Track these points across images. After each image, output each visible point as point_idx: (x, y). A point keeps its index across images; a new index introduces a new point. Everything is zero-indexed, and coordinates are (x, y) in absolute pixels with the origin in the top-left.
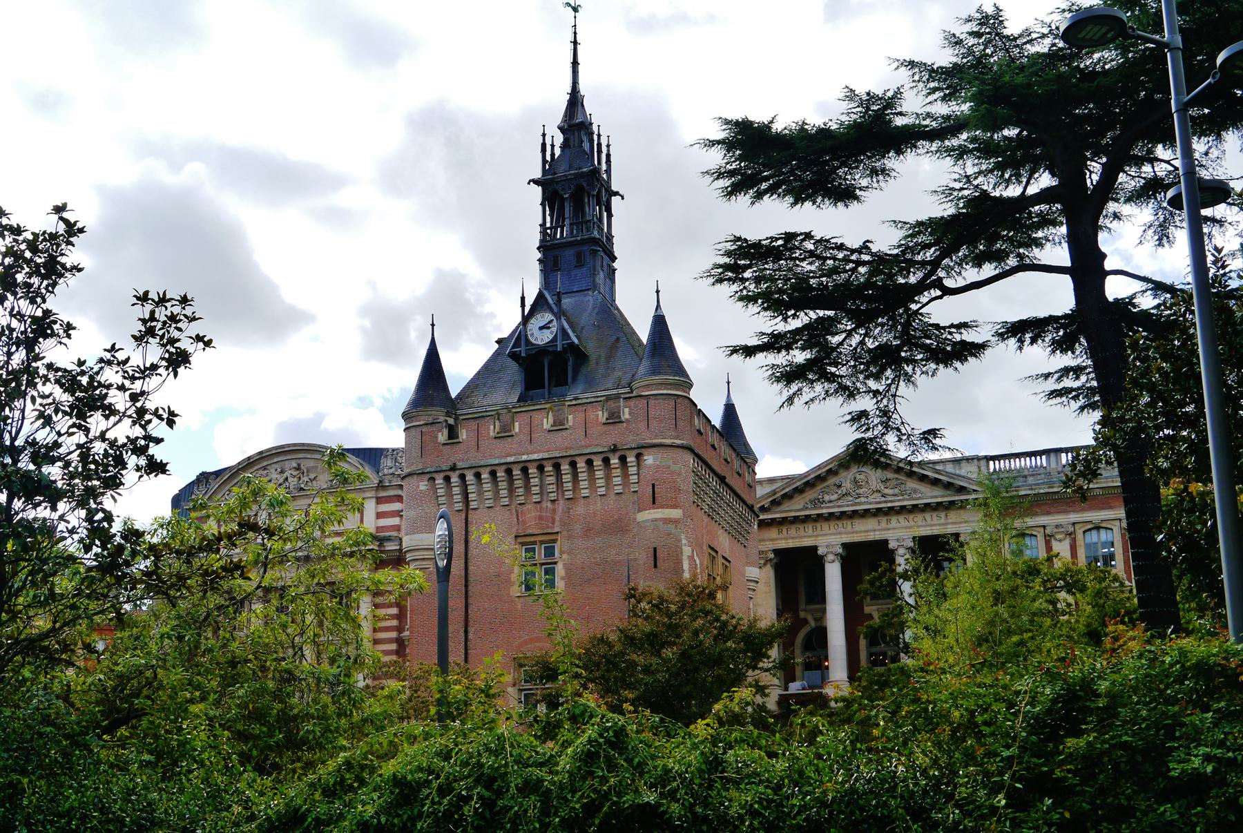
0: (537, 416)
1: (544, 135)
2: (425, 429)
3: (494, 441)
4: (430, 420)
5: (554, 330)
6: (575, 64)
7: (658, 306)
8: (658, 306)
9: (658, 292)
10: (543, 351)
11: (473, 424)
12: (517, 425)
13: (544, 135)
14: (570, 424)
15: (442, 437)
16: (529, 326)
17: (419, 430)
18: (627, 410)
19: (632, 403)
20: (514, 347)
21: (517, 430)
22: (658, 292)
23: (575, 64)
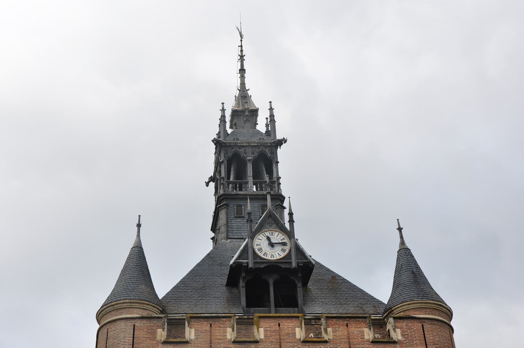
0: (287, 325)
1: (223, 110)
2: (138, 323)
3: (232, 346)
4: (145, 314)
5: (287, 248)
6: (242, 71)
7: (402, 243)
8: (402, 243)
9: (400, 229)
10: (273, 267)
11: (205, 326)
12: (262, 330)
13: (223, 110)
14: (331, 337)
15: (162, 334)
16: (256, 241)
17: (133, 322)
18: (398, 331)
19: (404, 324)
20: (239, 257)
21: (262, 336)
22: (400, 229)
23: (242, 71)
